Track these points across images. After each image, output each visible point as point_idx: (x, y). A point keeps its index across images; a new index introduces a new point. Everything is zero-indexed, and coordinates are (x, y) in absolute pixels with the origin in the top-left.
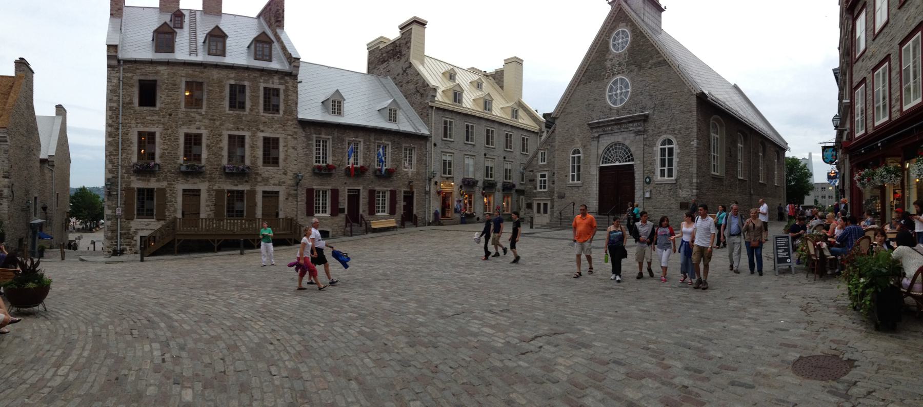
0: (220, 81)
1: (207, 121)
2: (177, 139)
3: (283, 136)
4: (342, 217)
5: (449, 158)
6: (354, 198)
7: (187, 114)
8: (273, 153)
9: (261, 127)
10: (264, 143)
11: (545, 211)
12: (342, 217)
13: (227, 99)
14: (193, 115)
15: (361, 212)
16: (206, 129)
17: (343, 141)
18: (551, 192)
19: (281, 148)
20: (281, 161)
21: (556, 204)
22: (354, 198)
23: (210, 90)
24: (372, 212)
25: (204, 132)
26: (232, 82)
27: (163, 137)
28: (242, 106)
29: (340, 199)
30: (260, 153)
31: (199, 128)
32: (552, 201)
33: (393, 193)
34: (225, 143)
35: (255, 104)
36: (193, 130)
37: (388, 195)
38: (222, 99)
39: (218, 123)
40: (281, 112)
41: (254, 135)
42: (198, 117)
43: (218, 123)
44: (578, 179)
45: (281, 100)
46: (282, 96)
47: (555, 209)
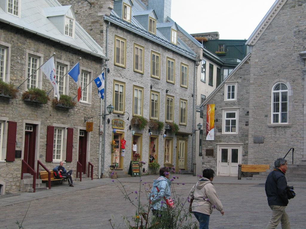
4: (18, 162)
5: (121, 90)
6: (31, 137)
11: (235, 159)
12: (18, 162)
15: (37, 158)
17: (23, 54)
18: (244, 136)
21: (250, 151)
22: (31, 137)
24: (49, 158)
29: (18, 136)
32: (246, 146)
33: (70, 132)
37: (64, 135)
44: (284, 119)
47: (250, 156)
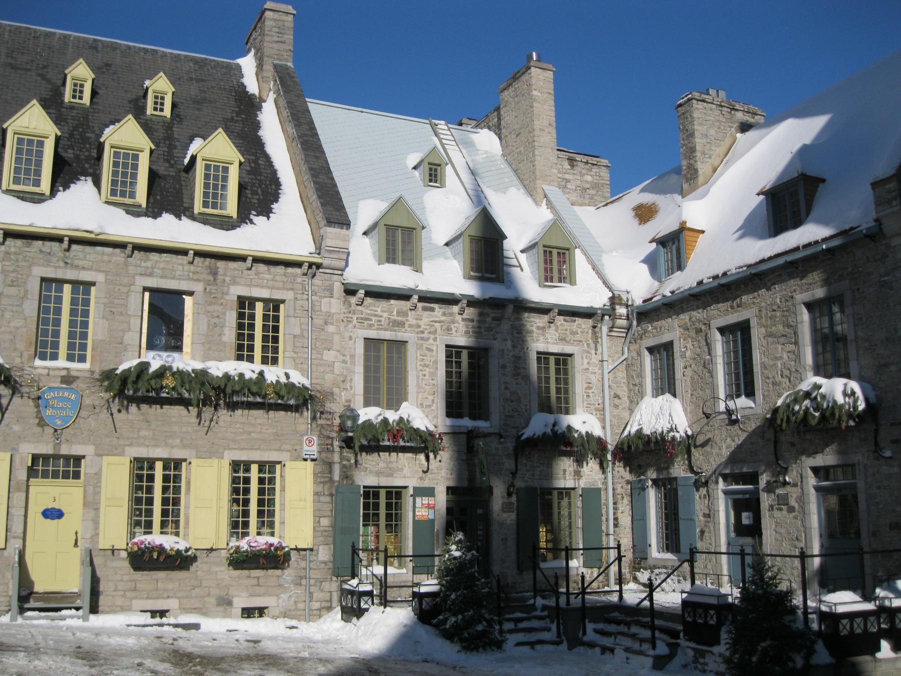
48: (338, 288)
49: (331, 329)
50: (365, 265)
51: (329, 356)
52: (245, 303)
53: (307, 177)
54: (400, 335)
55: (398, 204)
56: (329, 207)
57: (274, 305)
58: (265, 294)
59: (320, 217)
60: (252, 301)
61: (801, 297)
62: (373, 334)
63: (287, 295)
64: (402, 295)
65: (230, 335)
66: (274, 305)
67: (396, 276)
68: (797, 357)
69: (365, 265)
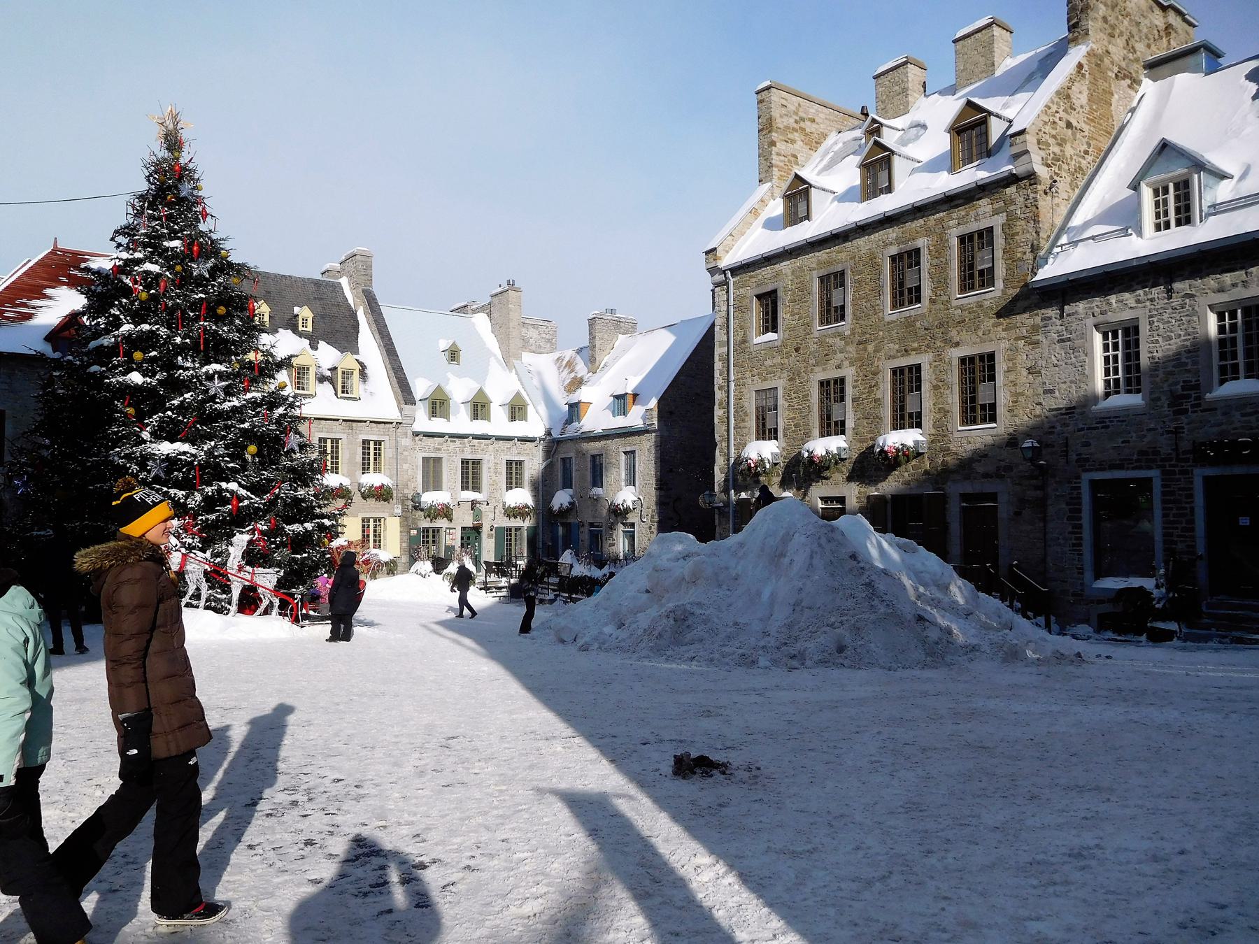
0: (872, 257)
1: (852, 349)
2: (806, 397)
3: (1004, 345)
7: (821, 342)
8: (983, 397)
9: (953, 333)
10: (963, 372)
13: (888, 290)
14: (830, 341)
16: (852, 364)
19: (1000, 378)
20: (1001, 411)
23: (859, 282)
25: (849, 373)
26: (894, 250)
27: (788, 396)
28: (915, 295)
30: (954, 400)
31: (839, 367)
34: (885, 391)
35: (941, 283)
36: (831, 374)
38: (879, 292)
39: (870, 348)
40: (999, 284)
41: (939, 357)
42: (840, 343)
43: (870, 348)
45: (999, 254)
46: (999, 241)
48: (410, 433)
49: (406, 453)
50: (423, 422)
51: (405, 466)
52: (366, 443)
53: (391, 372)
54: (439, 455)
55: (439, 389)
56: (405, 392)
57: (378, 443)
58: (375, 438)
59: (400, 398)
60: (368, 442)
61: (622, 449)
62: (426, 455)
63: (386, 438)
64: (441, 435)
65: (359, 458)
66: (378, 443)
67: (438, 425)
68: (619, 475)
69: (423, 422)
